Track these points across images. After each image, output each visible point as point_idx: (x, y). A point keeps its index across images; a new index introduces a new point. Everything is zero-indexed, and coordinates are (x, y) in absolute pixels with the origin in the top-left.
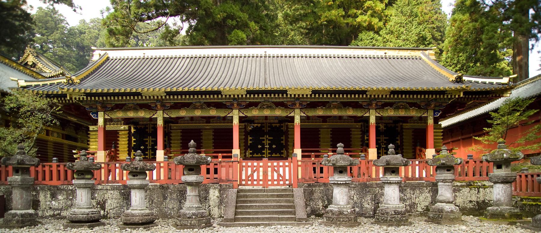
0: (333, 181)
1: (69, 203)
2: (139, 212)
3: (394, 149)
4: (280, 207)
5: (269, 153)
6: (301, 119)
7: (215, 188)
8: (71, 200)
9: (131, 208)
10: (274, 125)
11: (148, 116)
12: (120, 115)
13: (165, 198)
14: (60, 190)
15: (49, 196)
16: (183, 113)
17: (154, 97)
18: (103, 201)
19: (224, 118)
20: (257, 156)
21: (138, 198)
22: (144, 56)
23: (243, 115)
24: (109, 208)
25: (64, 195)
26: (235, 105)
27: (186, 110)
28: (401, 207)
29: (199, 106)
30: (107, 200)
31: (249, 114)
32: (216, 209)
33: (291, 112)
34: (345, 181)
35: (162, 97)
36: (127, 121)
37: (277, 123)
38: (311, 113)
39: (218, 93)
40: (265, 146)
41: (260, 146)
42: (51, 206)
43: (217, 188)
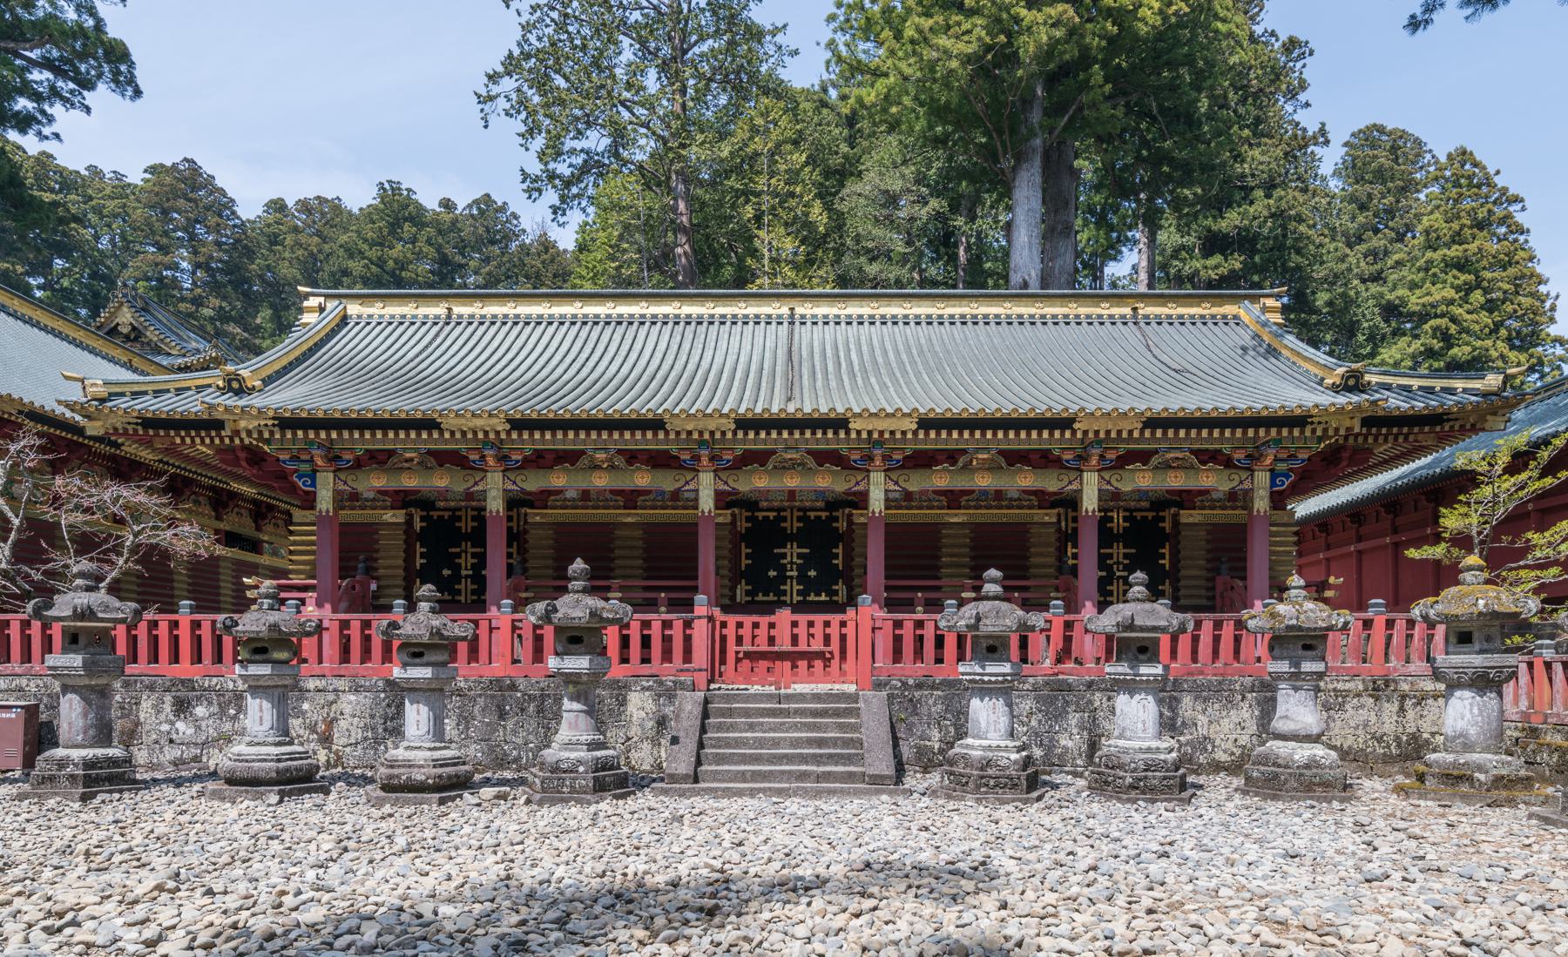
0: (970, 674)
1: (227, 726)
2: (428, 754)
3: (1147, 587)
4: (821, 743)
5: (799, 593)
6: (887, 500)
7: (644, 689)
8: (235, 718)
9: (405, 744)
10: (812, 514)
13: (502, 715)
14: (204, 694)
15: (168, 708)
18: (324, 720)
20: (765, 598)
23: (726, 488)
24: (344, 741)
25: (210, 703)
26: (705, 461)
27: (566, 470)
28: (1166, 748)
30: (336, 719)
32: (646, 746)
33: (859, 478)
36: (403, 499)
37: (821, 510)
38: (917, 482)
39: (656, 424)
40: (789, 574)
41: (772, 573)
42: (174, 736)
43: (648, 689)
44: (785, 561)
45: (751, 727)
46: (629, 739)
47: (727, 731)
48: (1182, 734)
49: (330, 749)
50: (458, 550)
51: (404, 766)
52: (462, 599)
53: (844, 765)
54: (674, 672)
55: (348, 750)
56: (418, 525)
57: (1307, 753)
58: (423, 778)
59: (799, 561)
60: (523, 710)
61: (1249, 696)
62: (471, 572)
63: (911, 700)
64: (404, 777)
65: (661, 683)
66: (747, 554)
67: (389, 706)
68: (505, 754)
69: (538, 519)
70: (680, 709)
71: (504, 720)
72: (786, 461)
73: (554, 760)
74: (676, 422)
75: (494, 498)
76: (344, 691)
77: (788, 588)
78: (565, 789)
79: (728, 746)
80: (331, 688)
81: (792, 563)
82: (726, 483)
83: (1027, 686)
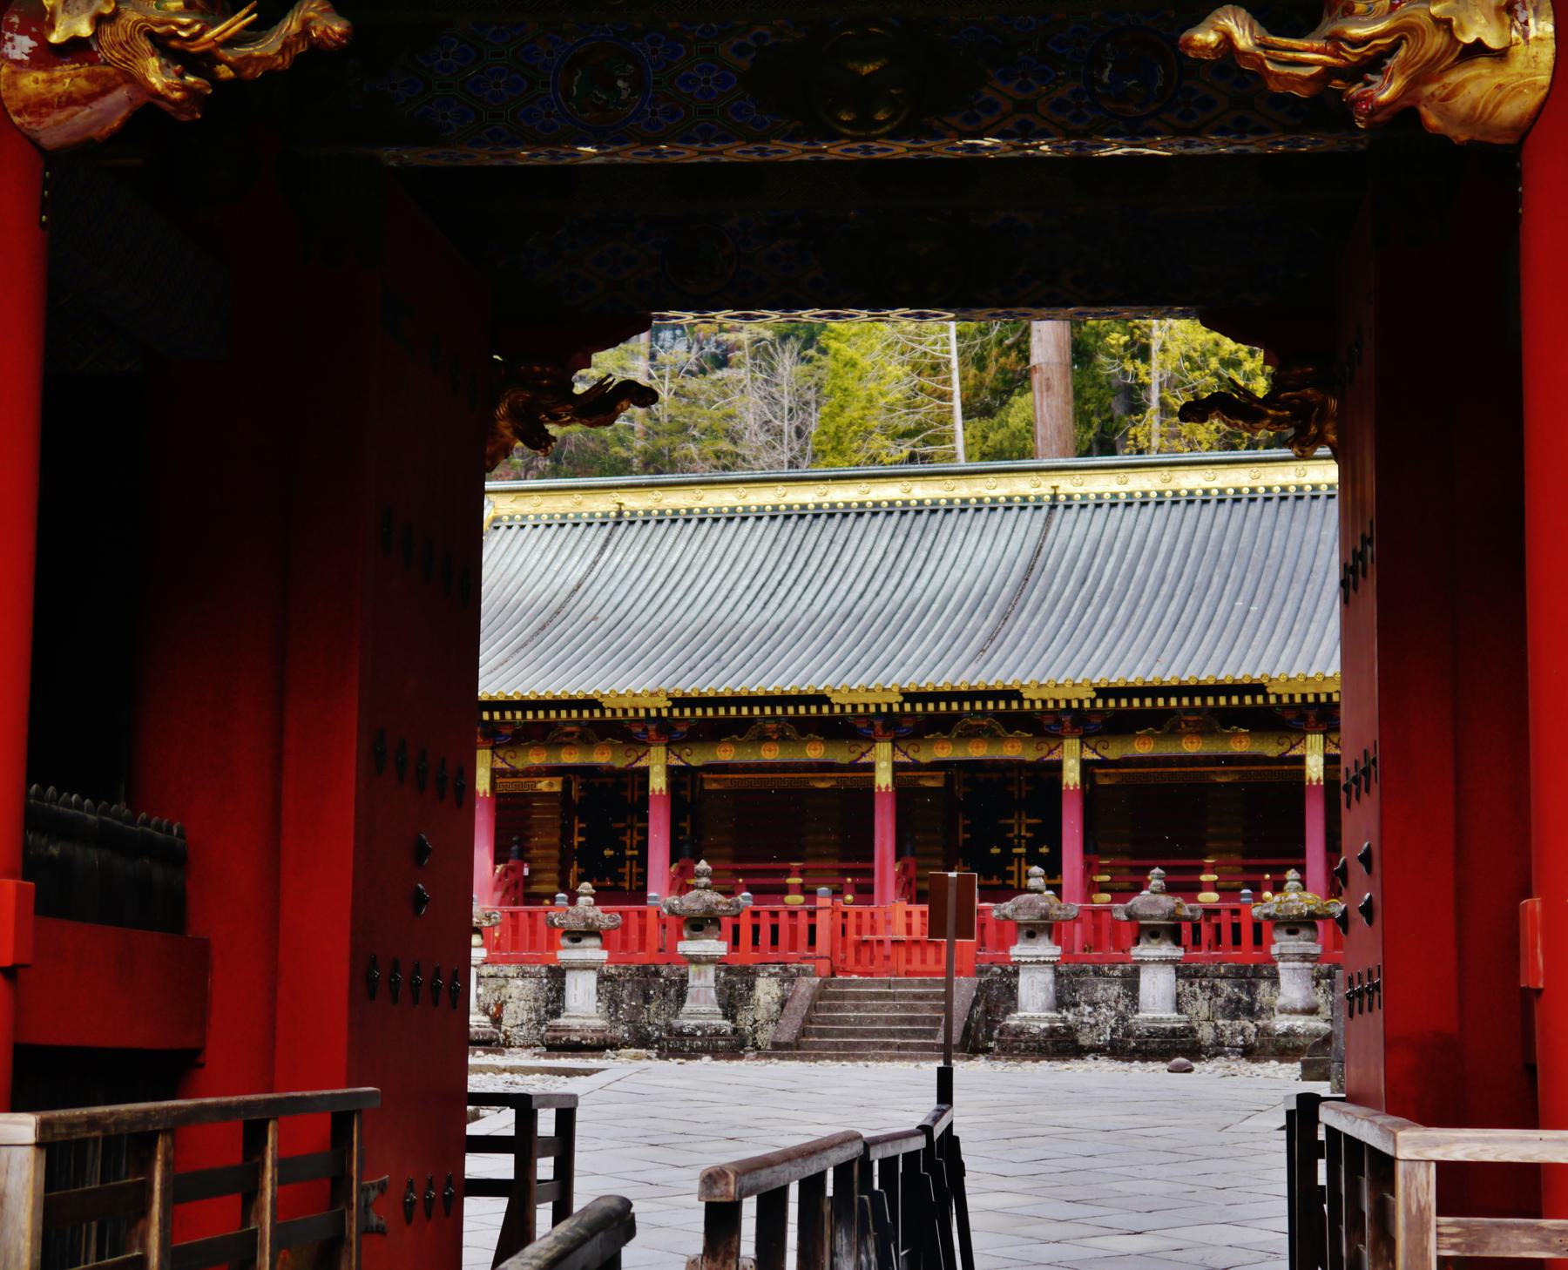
2: (582, 1021)
7: (771, 975)
9: (566, 1014)
11: (620, 763)
12: (536, 758)
13: (647, 999)
16: (725, 754)
17: (636, 711)
18: (496, 1004)
19: (853, 766)
21: (580, 992)
22: (620, 514)
24: (512, 1022)
27: (735, 743)
29: (773, 732)
30: (506, 1002)
31: (924, 757)
33: (1053, 746)
34: (1038, 956)
35: (659, 710)
40: (1016, 850)
41: (995, 851)
43: (775, 975)
44: (1011, 835)
45: (857, 1008)
46: (756, 1021)
47: (836, 1011)
48: (1259, 1018)
49: (500, 1029)
50: (622, 825)
51: (564, 1030)
52: (627, 885)
53: (926, 1038)
54: (798, 960)
55: (515, 1030)
56: (575, 793)
57: (1287, 1024)
58: (579, 1039)
59: (1029, 835)
60: (664, 994)
61: (1323, 982)
62: (636, 853)
63: (1008, 986)
64: (564, 1039)
65: (785, 970)
66: (965, 826)
67: (550, 990)
68: (649, 1035)
69: (715, 786)
70: (795, 992)
71: (648, 1003)
72: (971, 727)
73: (678, 1025)
74: (835, 695)
75: (658, 775)
76: (513, 977)
77: (1014, 868)
78: (686, 1049)
79: (833, 1023)
80: (501, 974)
81: (1020, 837)
82: (906, 754)
83: (1116, 973)
